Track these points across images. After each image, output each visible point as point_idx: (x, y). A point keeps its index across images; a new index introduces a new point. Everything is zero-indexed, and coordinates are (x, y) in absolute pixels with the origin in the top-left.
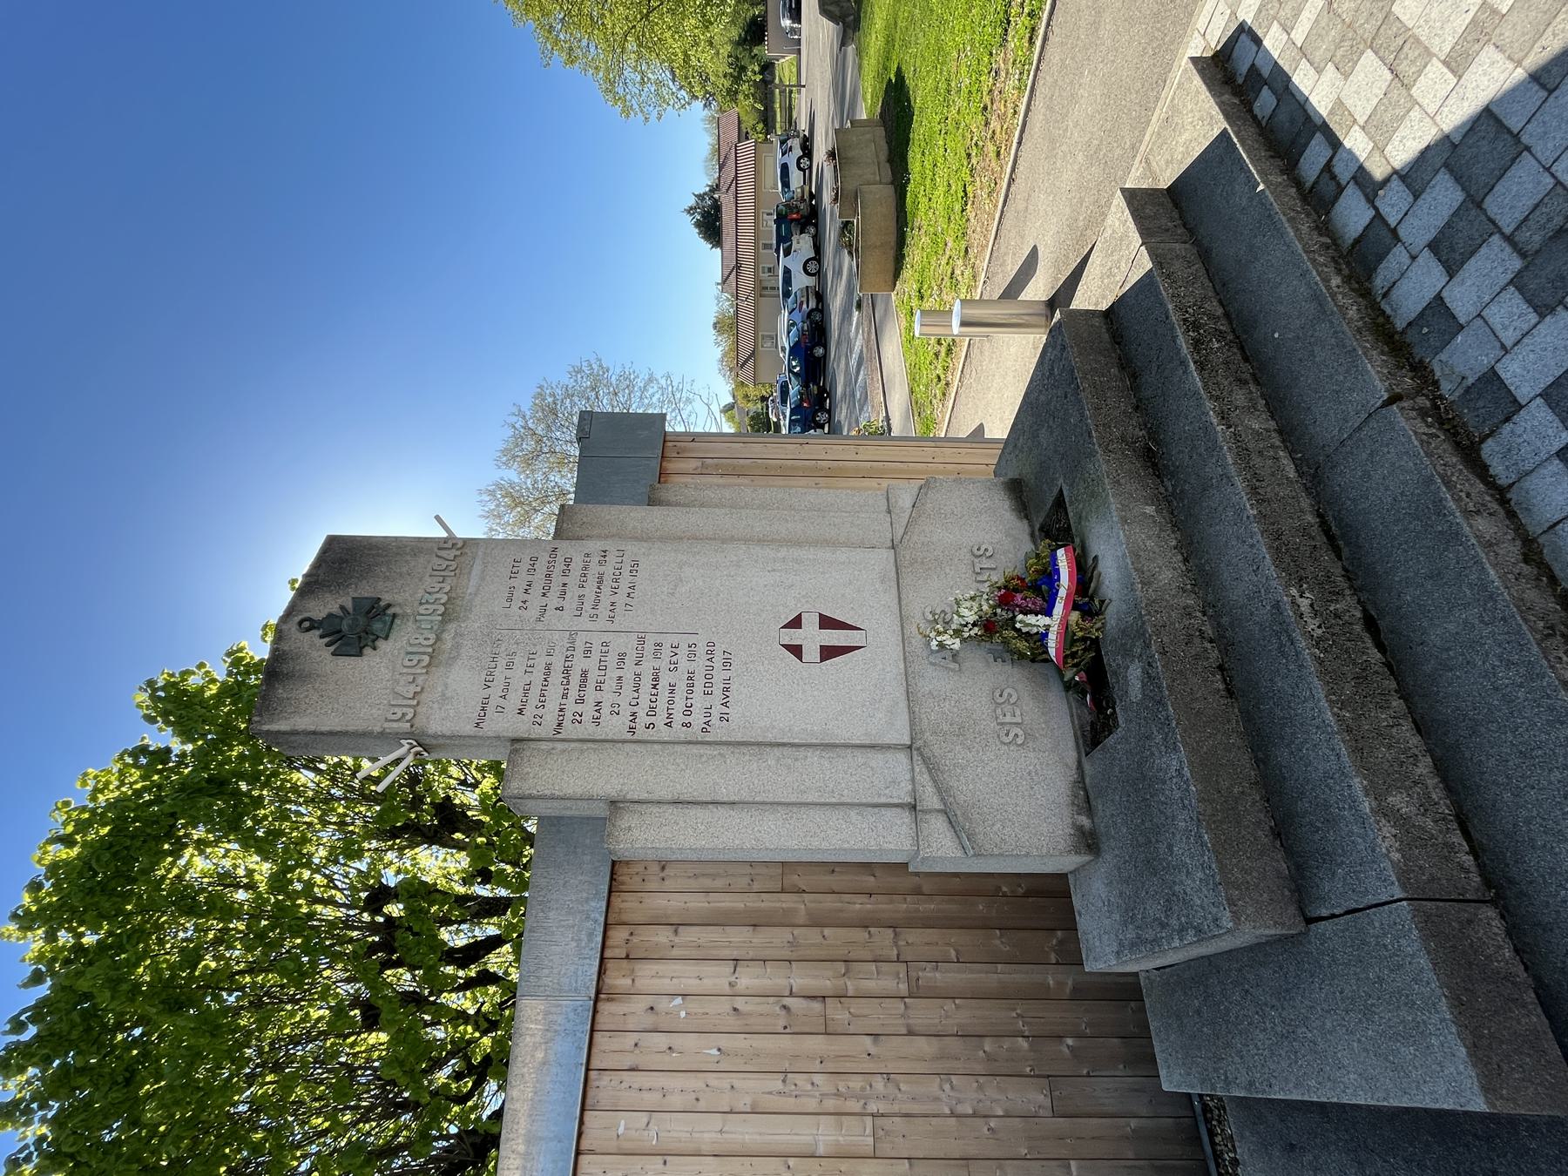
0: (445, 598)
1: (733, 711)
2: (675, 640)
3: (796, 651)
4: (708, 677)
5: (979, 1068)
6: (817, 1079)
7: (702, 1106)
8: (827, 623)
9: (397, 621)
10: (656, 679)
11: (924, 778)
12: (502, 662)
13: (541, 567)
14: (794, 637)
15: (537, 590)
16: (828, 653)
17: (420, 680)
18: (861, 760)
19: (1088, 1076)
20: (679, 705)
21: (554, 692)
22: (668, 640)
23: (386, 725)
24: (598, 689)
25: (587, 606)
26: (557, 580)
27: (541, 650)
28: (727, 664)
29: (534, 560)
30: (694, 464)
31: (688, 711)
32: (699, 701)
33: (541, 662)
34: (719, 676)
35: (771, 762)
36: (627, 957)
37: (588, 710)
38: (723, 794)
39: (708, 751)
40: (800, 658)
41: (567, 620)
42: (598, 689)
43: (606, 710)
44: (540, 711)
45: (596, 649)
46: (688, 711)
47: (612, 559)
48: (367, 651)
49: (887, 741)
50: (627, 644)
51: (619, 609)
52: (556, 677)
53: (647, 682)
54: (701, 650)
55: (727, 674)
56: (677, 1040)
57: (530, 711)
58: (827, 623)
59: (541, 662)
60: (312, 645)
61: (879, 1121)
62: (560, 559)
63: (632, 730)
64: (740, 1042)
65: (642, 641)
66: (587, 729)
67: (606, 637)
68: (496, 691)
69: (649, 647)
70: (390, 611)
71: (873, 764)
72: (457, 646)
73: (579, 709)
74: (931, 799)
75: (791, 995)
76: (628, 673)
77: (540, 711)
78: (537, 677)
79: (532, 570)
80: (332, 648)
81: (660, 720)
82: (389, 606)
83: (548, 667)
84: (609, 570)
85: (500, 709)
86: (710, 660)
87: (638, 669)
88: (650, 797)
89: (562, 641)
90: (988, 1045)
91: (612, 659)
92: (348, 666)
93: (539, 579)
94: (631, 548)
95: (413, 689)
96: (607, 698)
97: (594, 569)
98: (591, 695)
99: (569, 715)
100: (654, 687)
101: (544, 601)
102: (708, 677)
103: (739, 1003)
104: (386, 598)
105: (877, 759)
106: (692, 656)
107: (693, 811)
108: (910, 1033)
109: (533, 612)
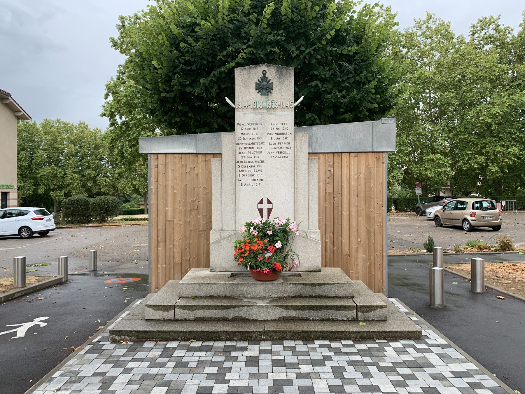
2: (263, 170)
3: (261, 202)
4: (253, 180)
5: (183, 247)
6: (181, 208)
8: (270, 211)
10: (252, 167)
11: (228, 234)
12: (255, 126)
14: (265, 201)
15: (277, 131)
16: (261, 211)
20: (245, 173)
21: (248, 141)
24: (249, 152)
26: (281, 136)
27: (259, 136)
28: (257, 184)
29: (287, 129)
30: (371, 164)
31: (243, 175)
32: (246, 178)
33: (256, 136)
34: (253, 183)
35: (231, 197)
37: (243, 150)
41: (268, 140)
42: (249, 152)
43: (243, 155)
45: (260, 150)
46: (243, 175)
48: (257, 91)
50: (262, 158)
51: (272, 155)
53: (251, 164)
54: (260, 178)
56: (188, 174)
57: (242, 136)
58: (270, 211)
59: (256, 136)
60: (258, 76)
62: (288, 136)
63: (238, 162)
66: (238, 151)
67: (263, 152)
69: (260, 164)
70: (269, 93)
72: (259, 114)
73: (243, 148)
74: (224, 235)
76: (254, 159)
78: (252, 136)
79: (283, 129)
80: (258, 82)
81: (241, 169)
82: (271, 93)
83: (254, 139)
84: (284, 150)
85: (242, 129)
87: (254, 162)
91: (257, 155)
93: (281, 131)
94: (291, 156)
96: (246, 155)
97: (284, 146)
98: (246, 151)
99: (241, 146)
101: (274, 134)
102: (253, 180)
103: (196, 189)
105: (233, 222)
106: (259, 175)
107: (220, 178)
109: (270, 131)
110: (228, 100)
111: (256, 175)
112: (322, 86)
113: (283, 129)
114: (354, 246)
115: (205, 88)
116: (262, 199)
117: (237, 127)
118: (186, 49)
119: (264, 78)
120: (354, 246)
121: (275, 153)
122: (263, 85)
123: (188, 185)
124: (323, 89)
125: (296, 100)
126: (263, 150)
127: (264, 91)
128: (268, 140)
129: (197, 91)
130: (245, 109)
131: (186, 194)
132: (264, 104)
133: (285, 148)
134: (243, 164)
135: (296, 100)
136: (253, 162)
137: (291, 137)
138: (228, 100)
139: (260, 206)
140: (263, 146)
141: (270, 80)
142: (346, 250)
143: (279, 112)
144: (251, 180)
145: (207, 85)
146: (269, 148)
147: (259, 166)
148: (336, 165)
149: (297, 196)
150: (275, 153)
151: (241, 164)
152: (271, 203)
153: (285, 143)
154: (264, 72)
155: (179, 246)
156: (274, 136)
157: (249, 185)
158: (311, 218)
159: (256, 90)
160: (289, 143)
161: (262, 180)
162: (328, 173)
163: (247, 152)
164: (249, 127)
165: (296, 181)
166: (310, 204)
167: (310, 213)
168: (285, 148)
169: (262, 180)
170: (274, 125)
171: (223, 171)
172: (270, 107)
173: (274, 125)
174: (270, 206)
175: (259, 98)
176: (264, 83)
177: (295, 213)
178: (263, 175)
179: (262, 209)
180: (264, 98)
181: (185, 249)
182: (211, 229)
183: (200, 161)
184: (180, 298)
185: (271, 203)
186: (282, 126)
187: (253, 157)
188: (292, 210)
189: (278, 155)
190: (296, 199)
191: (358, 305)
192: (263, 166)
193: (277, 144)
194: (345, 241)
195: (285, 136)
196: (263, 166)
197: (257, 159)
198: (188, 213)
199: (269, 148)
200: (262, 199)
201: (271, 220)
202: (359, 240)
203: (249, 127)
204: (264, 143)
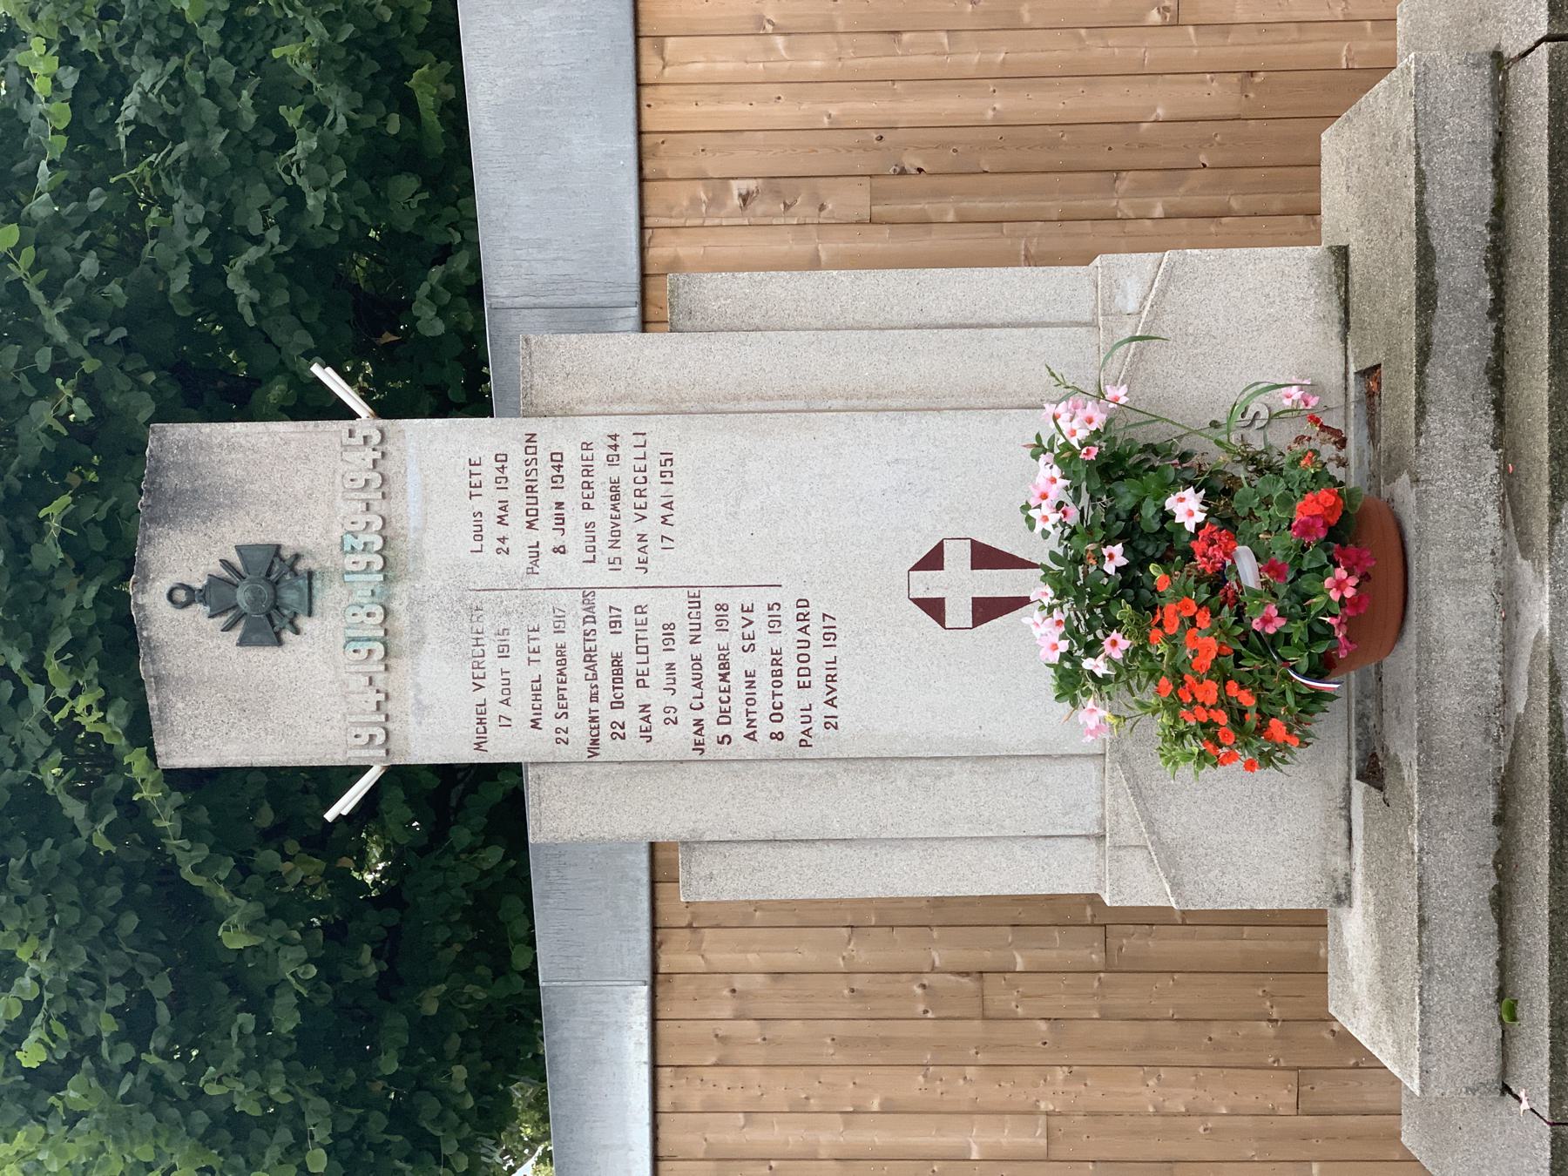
0: (378, 544)
1: (843, 712)
2: (746, 597)
3: (934, 608)
4: (803, 659)
5: (1203, 1059)
6: (971, 1072)
7: (814, 1104)
8: (985, 557)
9: (317, 584)
10: (724, 665)
12: (491, 649)
13: (516, 470)
14: (929, 584)
15: (517, 517)
16: (986, 610)
17: (379, 683)
18: (1030, 775)
19: (1356, 1066)
21: (578, 690)
22: (735, 599)
23: (350, 754)
24: (641, 683)
25: (602, 543)
27: (547, 624)
28: (830, 635)
29: (502, 459)
31: (777, 714)
32: (793, 700)
33: (548, 642)
34: (819, 657)
35: (902, 783)
36: (690, 926)
37: (630, 716)
38: (835, 829)
39: (809, 769)
40: (942, 622)
41: (570, 570)
42: (641, 683)
43: (657, 717)
44: (562, 723)
45: (628, 618)
46: (777, 714)
47: (627, 452)
48: (288, 635)
49: (1068, 750)
50: (672, 607)
52: (576, 668)
53: (711, 671)
54: (789, 613)
55: (829, 654)
56: (776, 1030)
57: (548, 722)
59: (548, 642)
60: (200, 630)
61: (1055, 1121)
63: (699, 746)
64: (864, 1028)
65: (695, 602)
66: (633, 746)
67: (640, 597)
68: (492, 693)
69: (708, 615)
70: (301, 566)
71: (1049, 780)
72: (417, 622)
73: (619, 716)
74: (1129, 826)
75: (933, 970)
76: (682, 654)
77: (562, 723)
79: (502, 481)
80: (236, 633)
81: (738, 729)
82: (297, 557)
83: (561, 650)
84: (625, 472)
85: (505, 722)
86: (803, 630)
87: (696, 650)
88: (735, 837)
89: (572, 604)
90: (1217, 1031)
92: (262, 656)
94: (661, 433)
95: (374, 698)
96: (657, 698)
97: (602, 475)
99: (605, 730)
100: (724, 678)
101: (534, 536)
102: (803, 659)
103: (860, 982)
104: (289, 544)
105: (1054, 774)
106: (775, 624)
107: (794, 851)
108: (1103, 1018)
109: (519, 559)
110: (345, 805)
111: (777, 642)
112: (258, 241)
113: (502, 481)
114: (1190, 45)
115: (278, 923)
116: (917, 601)
117: (496, 752)
118: (59, 1029)
119: (213, 596)
120: (1190, 45)
121: (642, 527)
122: (255, 601)
123: (840, 1029)
124: (274, 235)
125: (343, 412)
126: (626, 602)
127: (290, 597)
128: (570, 570)
129: (295, 967)
130: (390, 707)
131: (886, 1042)
132: (362, 594)
133: (614, 472)
134: (710, 715)
135: (343, 412)
136: (697, 660)
137: (554, 436)
138: (345, 805)
139: (959, 612)
140: (602, 601)
141: (225, 564)
142: (1215, 95)
143: (409, 510)
144: (804, 672)
145: (256, 909)
146: (615, 564)
147: (721, 625)
148: (712, 165)
149: (894, 394)
150: (642, 527)
151: (712, 730)
152: (939, 549)
153: (587, 471)
154: (181, 595)
155: (1199, 1083)
156: (547, 536)
157: (831, 678)
158: (1025, 312)
159: (279, 642)
160: (586, 446)
161: (803, 603)
162: (758, 207)
163: (642, 696)
164: (493, 682)
165: (809, 404)
166: (942, 314)
167: (998, 315)
168: (614, 472)
169: (803, 603)
170: (479, 536)
171: (751, 833)
172: (378, 563)
173: (479, 536)
174: (958, 555)
175: (331, 622)
176: (242, 597)
177: (994, 403)
178: (773, 596)
179: (977, 602)
180: (328, 596)
181: (1219, 1047)
182: (1094, 900)
183: (694, 962)
184: (1506, 1089)
185: (939, 549)
186: (489, 487)
187: (669, 657)
188: (976, 426)
189: (655, 511)
190: (912, 402)
191: (1543, 30)
192: (723, 596)
193: (589, 517)
194: (1160, 101)
195: (545, 471)
196: (723, 596)
197: (682, 635)
198: (1002, 1031)
199: (615, 564)
200: (917, 601)
201: (1039, 550)
202: (1155, 17)
203: (493, 682)
204: (588, 595)
